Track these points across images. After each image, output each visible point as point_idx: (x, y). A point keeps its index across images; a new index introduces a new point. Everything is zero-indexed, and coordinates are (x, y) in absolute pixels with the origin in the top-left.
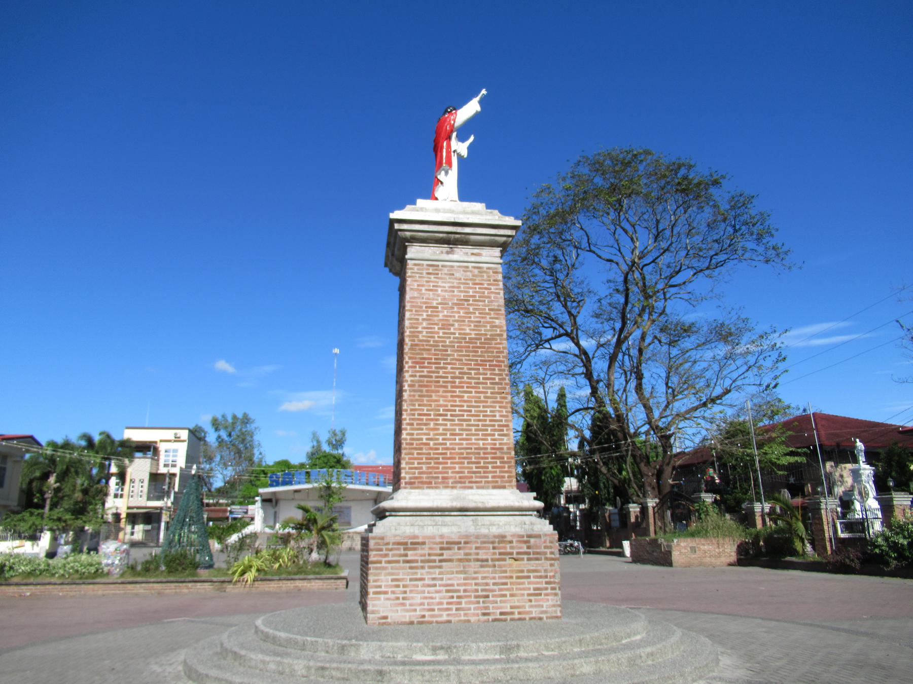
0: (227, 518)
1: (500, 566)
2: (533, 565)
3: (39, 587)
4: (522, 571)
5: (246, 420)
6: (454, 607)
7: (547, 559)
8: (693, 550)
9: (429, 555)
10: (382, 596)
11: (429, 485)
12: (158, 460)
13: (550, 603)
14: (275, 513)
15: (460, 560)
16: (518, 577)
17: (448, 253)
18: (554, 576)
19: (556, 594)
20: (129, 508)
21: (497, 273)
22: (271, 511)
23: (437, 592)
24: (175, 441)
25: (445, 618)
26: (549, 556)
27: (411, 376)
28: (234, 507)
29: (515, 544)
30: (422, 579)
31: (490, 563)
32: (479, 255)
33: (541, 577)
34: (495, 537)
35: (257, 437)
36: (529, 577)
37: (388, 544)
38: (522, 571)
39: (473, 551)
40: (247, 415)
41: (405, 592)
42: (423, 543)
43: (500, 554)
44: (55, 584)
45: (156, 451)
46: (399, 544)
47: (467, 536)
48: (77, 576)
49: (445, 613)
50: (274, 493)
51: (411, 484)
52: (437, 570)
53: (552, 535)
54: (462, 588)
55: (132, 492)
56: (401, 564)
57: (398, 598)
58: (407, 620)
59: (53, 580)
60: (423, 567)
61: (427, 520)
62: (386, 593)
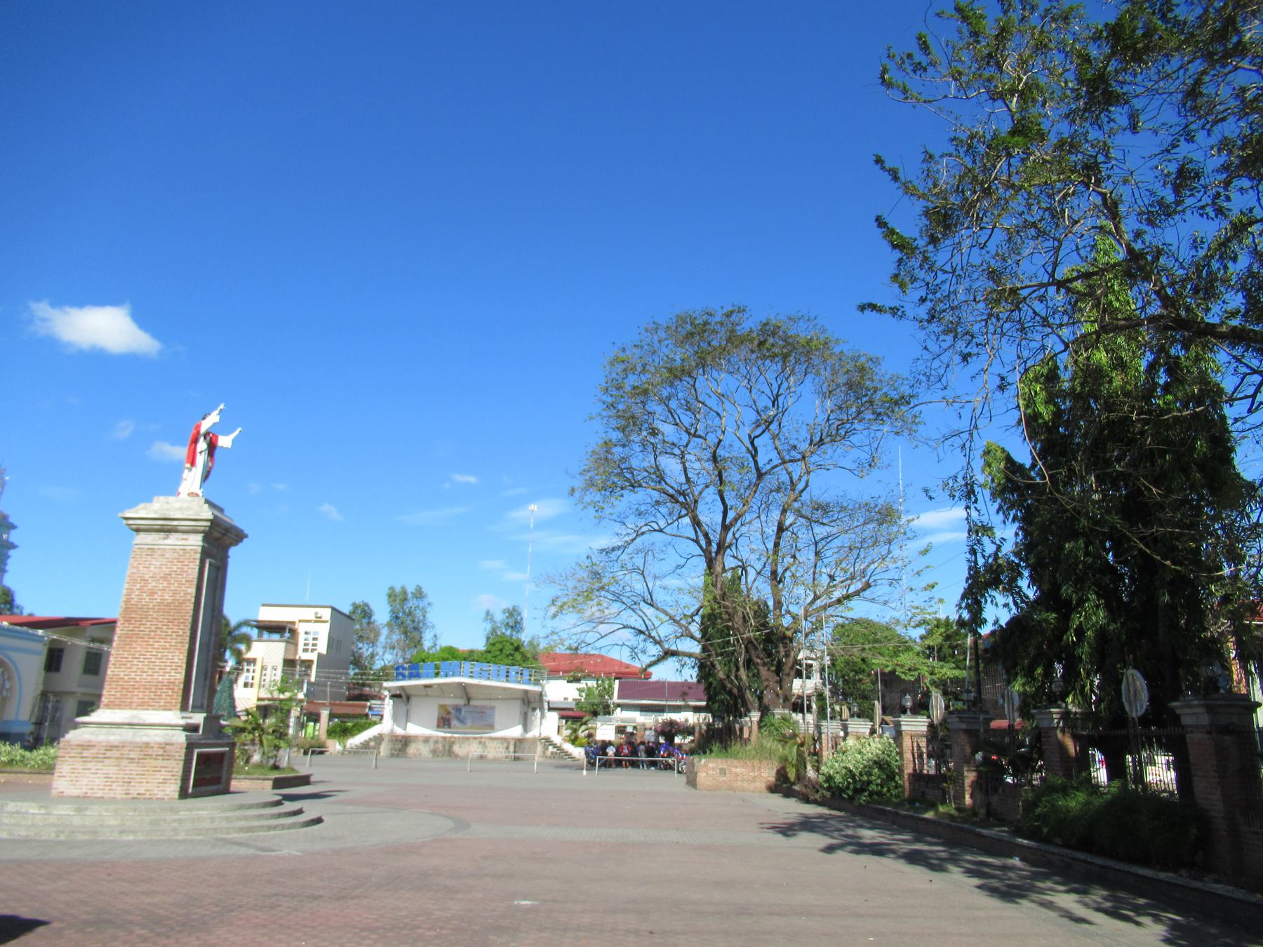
0: (367, 715)
1: (143, 763)
2: (165, 763)
3: (12, 775)
4: (157, 767)
5: (419, 594)
6: (107, 788)
7: (176, 760)
8: (723, 772)
9: (98, 754)
10: (63, 779)
11: (119, 706)
12: (296, 645)
13: (172, 789)
14: (408, 711)
15: (117, 758)
16: (154, 771)
17: (164, 539)
18: (177, 772)
19: (176, 784)
20: (259, 699)
21: (196, 553)
22: (403, 708)
23: (98, 778)
24: (316, 622)
25: (100, 795)
26: (177, 757)
27: (122, 630)
28: (374, 702)
29: (155, 749)
30: (89, 769)
31: (137, 761)
32: (186, 539)
33: (169, 771)
34: (143, 743)
35: (431, 617)
36: (160, 771)
37: (71, 745)
38: (157, 767)
39: (127, 752)
40: (420, 588)
41: (77, 777)
42: (94, 746)
43: (145, 755)
44: (25, 773)
45: (293, 632)
46: (79, 745)
47: (124, 743)
48: (43, 767)
49: (101, 792)
50: (402, 688)
51: (108, 706)
52: (101, 764)
53: (181, 744)
54: (115, 776)
55: (264, 680)
56: (78, 759)
57: (72, 781)
58: (76, 794)
59: (26, 770)
60: (91, 762)
61: (104, 731)
62: (65, 777)
